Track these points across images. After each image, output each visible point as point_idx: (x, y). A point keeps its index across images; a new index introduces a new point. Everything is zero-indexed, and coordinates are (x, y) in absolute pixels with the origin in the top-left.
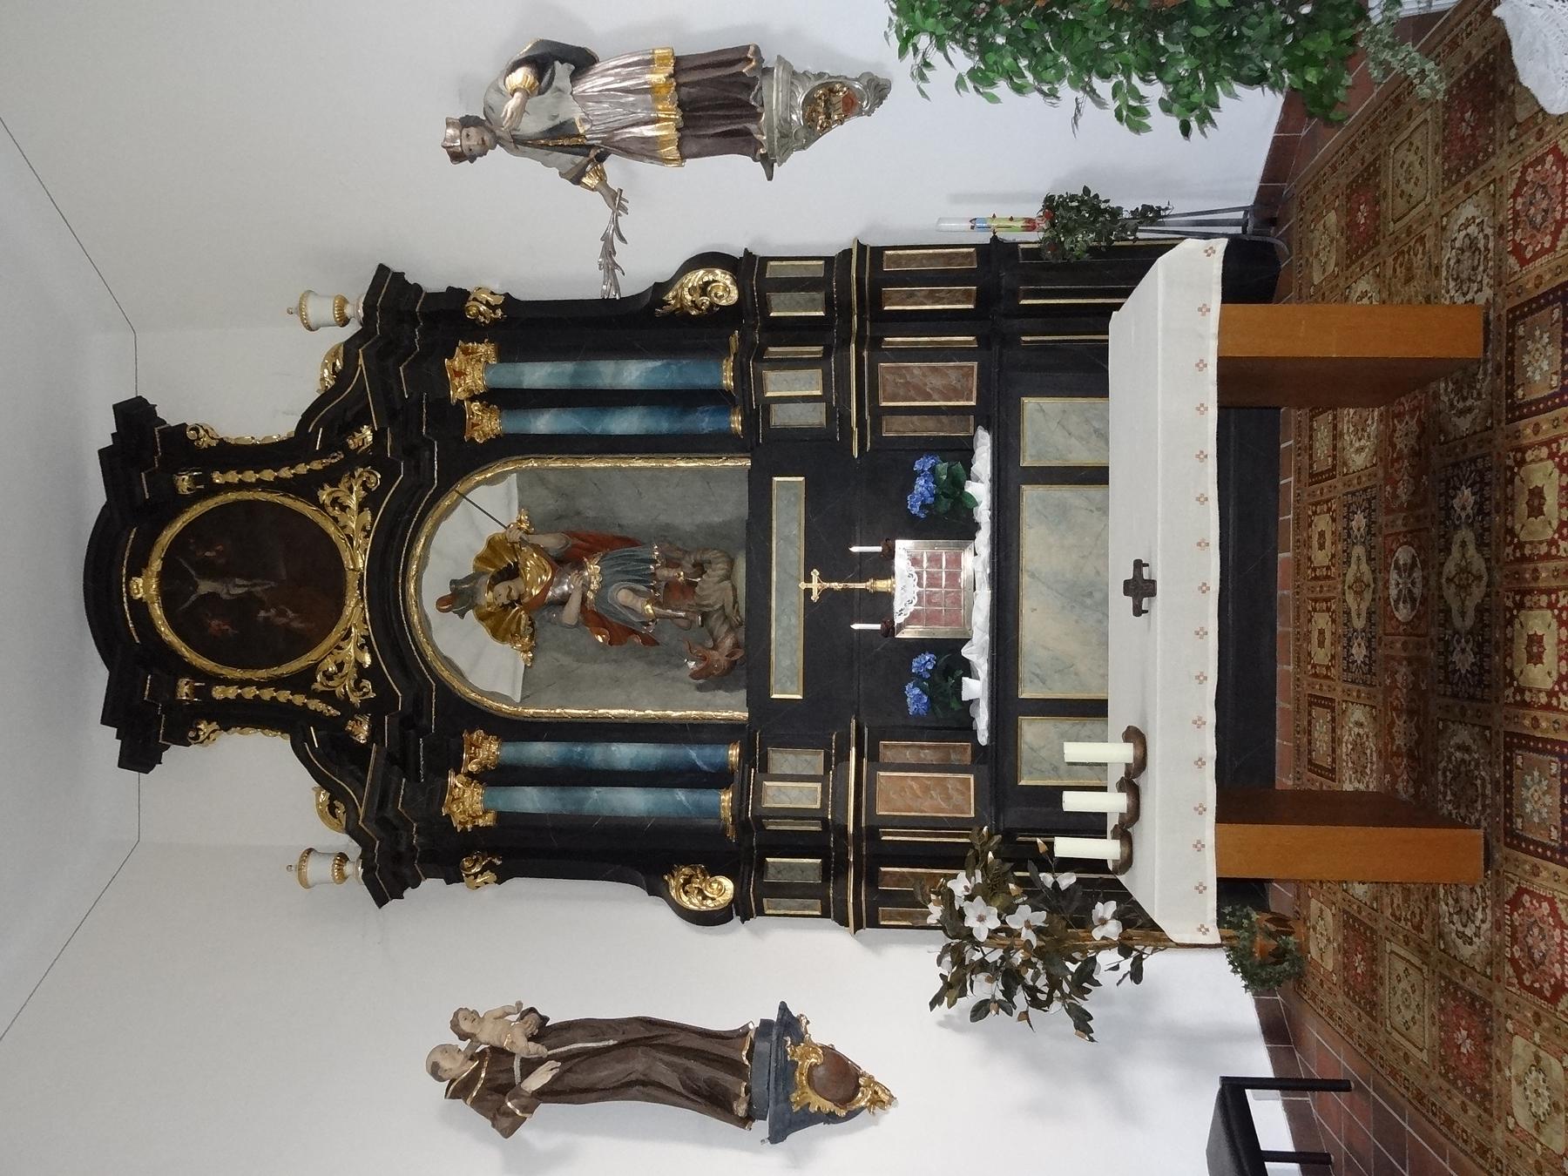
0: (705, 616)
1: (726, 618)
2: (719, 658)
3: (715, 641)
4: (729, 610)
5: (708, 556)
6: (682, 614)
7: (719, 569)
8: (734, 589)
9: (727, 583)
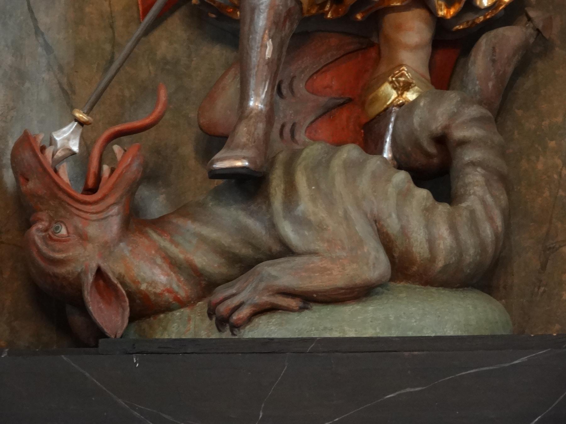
0: (249, 186)
1: (243, 264)
2: (89, 243)
3: (159, 224)
5: (478, 191)
6: (256, 103)
8: (361, 293)
9: (376, 265)
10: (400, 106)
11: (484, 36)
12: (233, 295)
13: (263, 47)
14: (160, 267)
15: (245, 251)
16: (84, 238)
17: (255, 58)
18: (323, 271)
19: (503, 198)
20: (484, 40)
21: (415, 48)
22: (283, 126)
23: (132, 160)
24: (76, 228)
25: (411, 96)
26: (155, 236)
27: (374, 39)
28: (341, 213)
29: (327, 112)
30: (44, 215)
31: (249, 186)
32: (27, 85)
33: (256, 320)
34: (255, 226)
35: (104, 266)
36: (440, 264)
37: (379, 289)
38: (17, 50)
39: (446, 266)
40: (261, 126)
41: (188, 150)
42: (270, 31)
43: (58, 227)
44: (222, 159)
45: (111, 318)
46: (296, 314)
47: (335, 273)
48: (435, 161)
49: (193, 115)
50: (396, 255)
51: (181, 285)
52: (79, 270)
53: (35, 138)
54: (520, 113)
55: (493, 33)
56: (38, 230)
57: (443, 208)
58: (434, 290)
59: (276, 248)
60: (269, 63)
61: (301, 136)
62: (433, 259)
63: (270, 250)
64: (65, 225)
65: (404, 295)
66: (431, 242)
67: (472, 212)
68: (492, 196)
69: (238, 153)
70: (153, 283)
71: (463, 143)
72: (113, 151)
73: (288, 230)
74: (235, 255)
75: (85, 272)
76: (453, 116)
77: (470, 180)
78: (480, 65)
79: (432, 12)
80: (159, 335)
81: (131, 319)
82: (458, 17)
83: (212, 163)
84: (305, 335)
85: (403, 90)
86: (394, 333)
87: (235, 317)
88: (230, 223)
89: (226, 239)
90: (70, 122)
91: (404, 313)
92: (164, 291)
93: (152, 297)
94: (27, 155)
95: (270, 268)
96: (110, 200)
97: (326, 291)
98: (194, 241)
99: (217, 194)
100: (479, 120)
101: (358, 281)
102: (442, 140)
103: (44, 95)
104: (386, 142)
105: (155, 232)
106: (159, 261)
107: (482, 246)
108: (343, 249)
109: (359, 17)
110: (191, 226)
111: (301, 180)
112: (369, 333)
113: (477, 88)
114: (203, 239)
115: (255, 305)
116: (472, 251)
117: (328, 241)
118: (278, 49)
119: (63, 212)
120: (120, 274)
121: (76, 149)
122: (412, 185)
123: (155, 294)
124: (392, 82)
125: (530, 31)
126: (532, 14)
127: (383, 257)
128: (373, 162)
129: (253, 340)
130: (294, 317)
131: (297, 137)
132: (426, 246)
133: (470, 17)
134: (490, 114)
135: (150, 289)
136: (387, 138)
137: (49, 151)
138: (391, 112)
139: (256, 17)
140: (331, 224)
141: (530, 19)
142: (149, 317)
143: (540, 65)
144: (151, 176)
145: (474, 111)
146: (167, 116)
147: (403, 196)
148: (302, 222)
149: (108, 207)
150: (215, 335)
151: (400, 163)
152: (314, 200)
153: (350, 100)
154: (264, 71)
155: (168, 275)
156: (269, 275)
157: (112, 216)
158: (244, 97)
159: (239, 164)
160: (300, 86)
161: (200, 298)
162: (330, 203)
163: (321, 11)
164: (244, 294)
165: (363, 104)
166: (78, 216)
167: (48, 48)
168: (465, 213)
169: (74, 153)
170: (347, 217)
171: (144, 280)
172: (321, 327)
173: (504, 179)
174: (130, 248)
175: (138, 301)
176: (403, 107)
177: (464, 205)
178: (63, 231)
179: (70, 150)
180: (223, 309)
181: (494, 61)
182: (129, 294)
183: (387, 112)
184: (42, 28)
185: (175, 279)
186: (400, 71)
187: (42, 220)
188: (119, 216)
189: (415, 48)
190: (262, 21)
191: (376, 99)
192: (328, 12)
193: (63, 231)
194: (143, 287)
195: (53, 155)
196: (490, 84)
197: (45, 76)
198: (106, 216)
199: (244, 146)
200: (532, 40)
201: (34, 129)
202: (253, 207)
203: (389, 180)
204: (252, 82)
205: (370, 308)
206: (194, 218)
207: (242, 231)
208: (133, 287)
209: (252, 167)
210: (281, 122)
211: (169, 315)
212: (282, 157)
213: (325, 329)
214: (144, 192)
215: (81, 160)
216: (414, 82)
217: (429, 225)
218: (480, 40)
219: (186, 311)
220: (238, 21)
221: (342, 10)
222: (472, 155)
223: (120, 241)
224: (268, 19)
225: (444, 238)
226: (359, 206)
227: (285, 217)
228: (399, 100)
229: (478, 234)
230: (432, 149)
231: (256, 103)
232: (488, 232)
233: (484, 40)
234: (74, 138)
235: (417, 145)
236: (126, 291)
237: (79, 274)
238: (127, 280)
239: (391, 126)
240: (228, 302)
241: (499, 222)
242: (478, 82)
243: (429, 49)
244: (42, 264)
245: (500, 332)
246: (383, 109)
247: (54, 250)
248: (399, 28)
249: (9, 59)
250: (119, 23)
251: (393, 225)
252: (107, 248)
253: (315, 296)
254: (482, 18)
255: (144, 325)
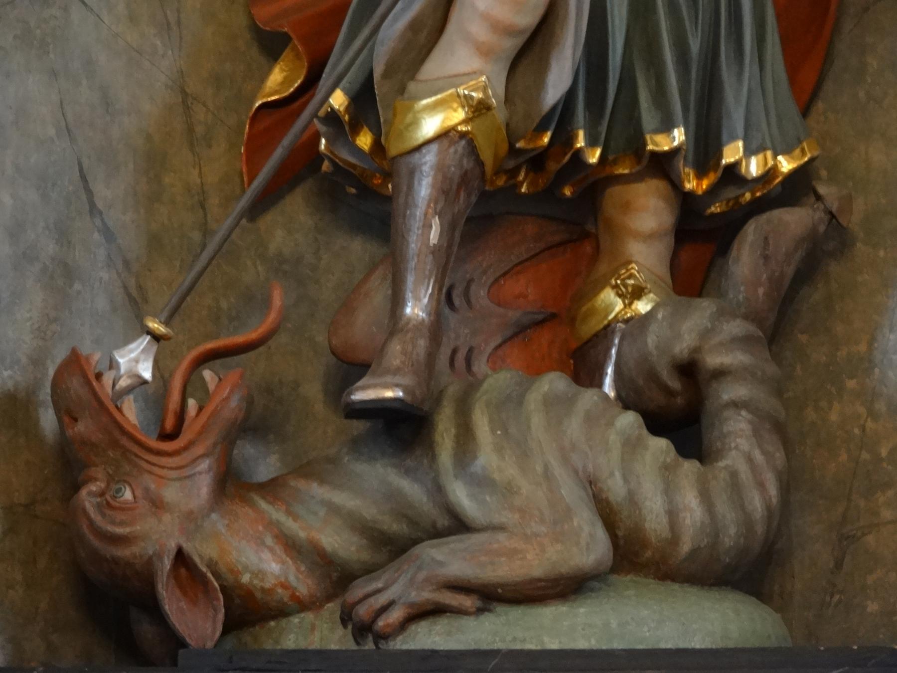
0: (403, 429)
1: (392, 548)
2: (166, 512)
3: (271, 489)
4: (452, 559)
5: (741, 442)
6: (415, 309)
7: (667, 494)
8: (568, 587)
9: (590, 547)
10: (627, 321)
11: (750, 222)
12: (378, 591)
13: (425, 228)
14: (271, 550)
15: (395, 527)
16: (157, 505)
17: (414, 244)
18: (513, 553)
19: (780, 456)
20: (753, 227)
21: (649, 237)
22: (454, 352)
23: (231, 391)
24: (147, 490)
25: (643, 307)
26: (263, 505)
27: (590, 227)
28: (539, 469)
29: (520, 332)
30: (99, 472)
31: (403, 429)
32: (77, 286)
33: (413, 628)
34: (413, 490)
35: (188, 547)
36: (686, 547)
37: (595, 584)
38: (63, 235)
39: (695, 552)
40: (422, 343)
41: (313, 390)
42: (436, 203)
43: (121, 489)
44: (364, 388)
45: (197, 624)
46: (472, 618)
47: (529, 557)
48: (679, 400)
49: (321, 338)
50: (620, 533)
51: (301, 576)
52: (151, 553)
53: (87, 359)
54: (803, 338)
55: (765, 217)
56: (90, 494)
57: (690, 467)
58: (676, 586)
59: (443, 522)
60: (435, 251)
61: (481, 366)
62: (674, 540)
63: (434, 525)
64: (130, 485)
65: (631, 592)
66: (672, 514)
67: (734, 475)
68: (764, 452)
69: (389, 379)
70: (259, 574)
71: (720, 374)
72: (203, 379)
73: (461, 495)
74: (382, 533)
75: (160, 557)
76: (706, 334)
77: (731, 429)
78: (746, 263)
79: (676, 185)
80: (268, 645)
81: (226, 631)
82: (713, 192)
83: (350, 393)
84: (485, 647)
85: (631, 301)
86: (617, 645)
87: (380, 623)
88: (376, 485)
89: (369, 511)
90: (139, 336)
91: (632, 619)
92: (276, 585)
93: (259, 595)
94: (75, 384)
95: (434, 550)
96: (199, 450)
97: (516, 584)
98: (322, 513)
99: (356, 445)
100: (745, 341)
101: (564, 569)
102: (689, 369)
103: (101, 303)
104: (607, 374)
105: (264, 498)
106: (269, 541)
107: (747, 523)
108: (542, 521)
109: (568, 192)
110: (317, 490)
111: (481, 422)
112: (582, 644)
113: (741, 297)
114: (334, 510)
115: (411, 605)
116: (732, 531)
117: (521, 510)
118: (448, 230)
119: (127, 468)
120: (211, 559)
121: (147, 375)
122: (645, 431)
123: (262, 589)
124: (616, 287)
125: (820, 215)
126: (822, 190)
127: (601, 534)
128: (588, 396)
129: (409, 652)
130: (469, 623)
131: (475, 369)
132: (665, 520)
133: (731, 192)
134: (761, 334)
135: (256, 582)
136: (608, 368)
137: (108, 379)
138: (613, 332)
139: (416, 183)
140: (525, 486)
141: (819, 198)
142: (253, 624)
143: (834, 268)
144: (257, 423)
145: (736, 327)
146: (283, 338)
147: (631, 446)
148: (482, 483)
149: (194, 461)
150: (352, 646)
151: (627, 399)
152: (499, 449)
153: (552, 317)
154: (429, 263)
155: (283, 563)
156: (433, 559)
157: (200, 473)
158: (397, 301)
159: (389, 394)
160: (480, 294)
161: (329, 598)
162: (524, 454)
163: (512, 182)
164: (395, 590)
165: (572, 321)
166: (150, 472)
167: (108, 234)
168: (723, 475)
169: (145, 382)
170: (547, 474)
171: (246, 568)
172: (509, 638)
173: (779, 429)
174: (226, 522)
175: (237, 601)
176: (631, 323)
177: (721, 464)
178: (128, 495)
179: (139, 377)
180: (363, 611)
181: (766, 258)
182: (224, 589)
183: (607, 331)
184: (100, 205)
185: (292, 569)
186: (628, 270)
187: (96, 480)
188: (211, 474)
189: (649, 237)
190: (425, 188)
191: (593, 312)
192: (522, 183)
193: (128, 495)
194: (246, 579)
195: (114, 385)
196: (761, 291)
197: (105, 275)
198: (193, 472)
199: (397, 371)
200: (822, 228)
201: (85, 349)
202: (409, 463)
203: (610, 424)
204: (410, 279)
205: (582, 610)
206: (322, 481)
207: (393, 495)
208: (230, 578)
209: (409, 399)
210: (452, 347)
211: (284, 622)
212: (453, 390)
213: (515, 639)
214: (246, 450)
215: (154, 393)
216: (649, 286)
217: (669, 490)
218: (745, 227)
219: (309, 616)
220: (389, 199)
221: (542, 182)
222: (731, 391)
223: (212, 510)
224: (433, 186)
225: (692, 510)
226: (565, 460)
227: (456, 477)
228: (626, 313)
229: (742, 507)
230: (675, 384)
231: (415, 309)
232: (756, 504)
233: (753, 227)
234: (145, 360)
235: (653, 376)
236: (220, 585)
237: (150, 558)
238: (223, 568)
239: (614, 351)
240: (372, 600)
241: (773, 491)
242: (742, 288)
243: (670, 240)
244: (96, 543)
245: (773, 643)
246: (602, 326)
247: (113, 523)
248: (626, 207)
249: (50, 248)
250: (214, 201)
251: (616, 488)
252: (192, 521)
253: (500, 591)
254: (748, 196)
255: (246, 637)
